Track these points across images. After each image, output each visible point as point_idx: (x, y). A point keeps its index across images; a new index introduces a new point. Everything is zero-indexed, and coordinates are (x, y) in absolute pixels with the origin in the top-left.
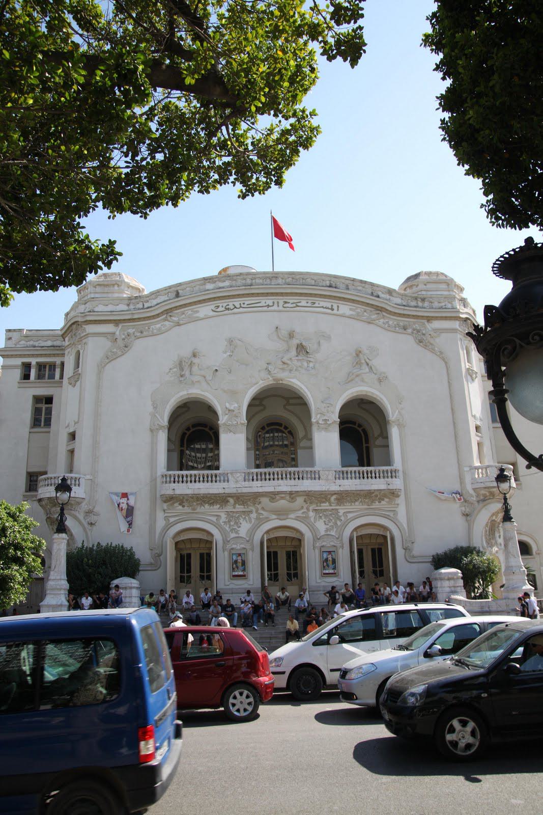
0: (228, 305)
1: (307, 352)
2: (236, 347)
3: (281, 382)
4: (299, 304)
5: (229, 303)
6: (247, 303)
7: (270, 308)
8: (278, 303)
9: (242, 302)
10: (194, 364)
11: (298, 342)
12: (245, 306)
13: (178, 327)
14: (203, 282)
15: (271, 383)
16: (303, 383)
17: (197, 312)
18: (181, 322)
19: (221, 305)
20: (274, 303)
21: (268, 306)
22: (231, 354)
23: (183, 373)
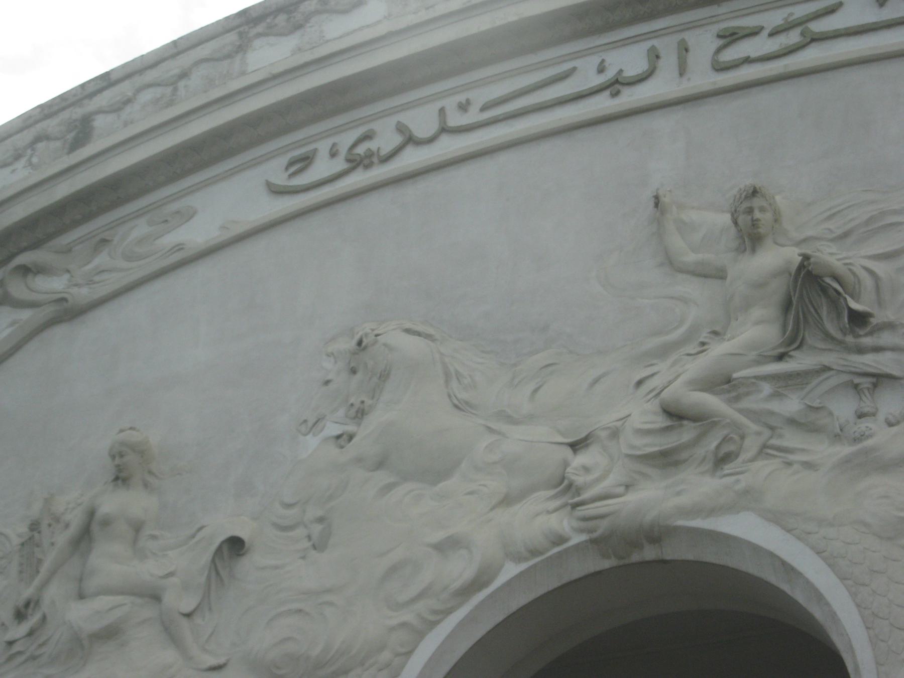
0: (367, 137)
1: (859, 319)
2: (384, 376)
3: (649, 553)
4: (818, 26)
5: (376, 126)
6: (481, 96)
7: (631, 97)
8: (684, 49)
9: (450, 103)
10: (106, 522)
11: (792, 255)
12: (473, 116)
13: (59, 332)
14: (232, 37)
15: (578, 569)
16: (802, 537)
17: (188, 215)
18: (83, 294)
19: (323, 147)
20: (654, 56)
21: (616, 85)
22: (351, 428)
23: (28, 592)
